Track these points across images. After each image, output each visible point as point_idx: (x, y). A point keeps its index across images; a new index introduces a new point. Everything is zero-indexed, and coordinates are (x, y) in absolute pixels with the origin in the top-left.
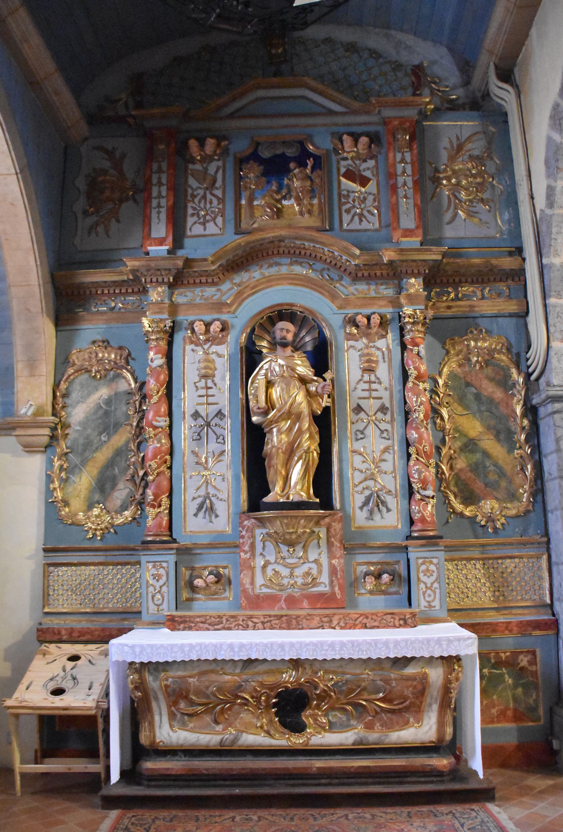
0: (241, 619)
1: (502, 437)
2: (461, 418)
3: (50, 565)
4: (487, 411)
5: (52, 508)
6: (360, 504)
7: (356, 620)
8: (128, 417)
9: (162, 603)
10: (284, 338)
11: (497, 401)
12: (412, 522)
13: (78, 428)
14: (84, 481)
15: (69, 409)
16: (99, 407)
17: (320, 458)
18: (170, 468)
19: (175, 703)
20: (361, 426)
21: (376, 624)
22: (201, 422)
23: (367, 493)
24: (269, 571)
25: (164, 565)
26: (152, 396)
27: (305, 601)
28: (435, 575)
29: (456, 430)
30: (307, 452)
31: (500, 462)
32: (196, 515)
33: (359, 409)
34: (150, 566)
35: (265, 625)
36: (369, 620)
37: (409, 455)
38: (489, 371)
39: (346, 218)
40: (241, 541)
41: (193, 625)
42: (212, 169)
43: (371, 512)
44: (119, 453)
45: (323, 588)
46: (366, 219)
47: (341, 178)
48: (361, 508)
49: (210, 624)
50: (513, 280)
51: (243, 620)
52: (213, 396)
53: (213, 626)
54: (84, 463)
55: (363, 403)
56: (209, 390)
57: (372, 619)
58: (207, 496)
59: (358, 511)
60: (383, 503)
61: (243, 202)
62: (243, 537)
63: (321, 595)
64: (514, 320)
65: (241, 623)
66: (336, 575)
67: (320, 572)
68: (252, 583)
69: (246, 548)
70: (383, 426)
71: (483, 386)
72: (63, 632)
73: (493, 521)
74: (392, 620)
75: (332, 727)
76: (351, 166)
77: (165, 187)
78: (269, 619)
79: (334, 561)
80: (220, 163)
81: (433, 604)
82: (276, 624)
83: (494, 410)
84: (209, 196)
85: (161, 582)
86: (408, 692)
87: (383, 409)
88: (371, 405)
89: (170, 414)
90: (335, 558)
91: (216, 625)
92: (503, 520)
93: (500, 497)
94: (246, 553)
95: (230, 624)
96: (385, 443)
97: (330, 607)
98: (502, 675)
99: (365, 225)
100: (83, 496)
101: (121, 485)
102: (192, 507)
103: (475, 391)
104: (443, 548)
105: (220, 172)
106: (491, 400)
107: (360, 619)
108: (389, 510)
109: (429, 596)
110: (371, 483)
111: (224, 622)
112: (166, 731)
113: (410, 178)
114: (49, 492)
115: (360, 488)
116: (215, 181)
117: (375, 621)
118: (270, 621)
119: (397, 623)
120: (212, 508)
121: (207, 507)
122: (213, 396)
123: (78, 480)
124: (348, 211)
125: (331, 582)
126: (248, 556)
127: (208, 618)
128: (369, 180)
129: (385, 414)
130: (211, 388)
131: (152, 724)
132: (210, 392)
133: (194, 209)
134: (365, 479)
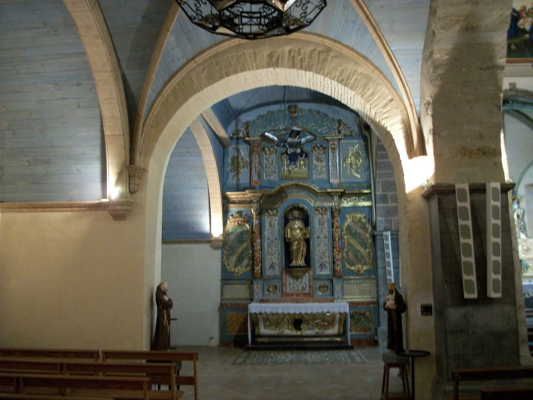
3: (223, 284)
5: (224, 267)
12: (334, 272)
14: (234, 258)
16: (238, 235)
19: (266, 322)
20: (319, 242)
24: (291, 286)
29: (348, 243)
30: (303, 250)
33: (318, 237)
37: (333, 252)
38: (360, 224)
42: (272, 156)
43: (322, 269)
44: (245, 250)
45: (307, 290)
54: (234, 253)
55: (320, 236)
58: (272, 264)
60: (326, 266)
75: (309, 329)
84: (271, 166)
86: (330, 320)
87: (326, 237)
88: (322, 236)
97: (309, 296)
98: (361, 319)
99: (321, 177)
106: (359, 234)
112: (263, 330)
128: (322, 161)
131: (259, 328)
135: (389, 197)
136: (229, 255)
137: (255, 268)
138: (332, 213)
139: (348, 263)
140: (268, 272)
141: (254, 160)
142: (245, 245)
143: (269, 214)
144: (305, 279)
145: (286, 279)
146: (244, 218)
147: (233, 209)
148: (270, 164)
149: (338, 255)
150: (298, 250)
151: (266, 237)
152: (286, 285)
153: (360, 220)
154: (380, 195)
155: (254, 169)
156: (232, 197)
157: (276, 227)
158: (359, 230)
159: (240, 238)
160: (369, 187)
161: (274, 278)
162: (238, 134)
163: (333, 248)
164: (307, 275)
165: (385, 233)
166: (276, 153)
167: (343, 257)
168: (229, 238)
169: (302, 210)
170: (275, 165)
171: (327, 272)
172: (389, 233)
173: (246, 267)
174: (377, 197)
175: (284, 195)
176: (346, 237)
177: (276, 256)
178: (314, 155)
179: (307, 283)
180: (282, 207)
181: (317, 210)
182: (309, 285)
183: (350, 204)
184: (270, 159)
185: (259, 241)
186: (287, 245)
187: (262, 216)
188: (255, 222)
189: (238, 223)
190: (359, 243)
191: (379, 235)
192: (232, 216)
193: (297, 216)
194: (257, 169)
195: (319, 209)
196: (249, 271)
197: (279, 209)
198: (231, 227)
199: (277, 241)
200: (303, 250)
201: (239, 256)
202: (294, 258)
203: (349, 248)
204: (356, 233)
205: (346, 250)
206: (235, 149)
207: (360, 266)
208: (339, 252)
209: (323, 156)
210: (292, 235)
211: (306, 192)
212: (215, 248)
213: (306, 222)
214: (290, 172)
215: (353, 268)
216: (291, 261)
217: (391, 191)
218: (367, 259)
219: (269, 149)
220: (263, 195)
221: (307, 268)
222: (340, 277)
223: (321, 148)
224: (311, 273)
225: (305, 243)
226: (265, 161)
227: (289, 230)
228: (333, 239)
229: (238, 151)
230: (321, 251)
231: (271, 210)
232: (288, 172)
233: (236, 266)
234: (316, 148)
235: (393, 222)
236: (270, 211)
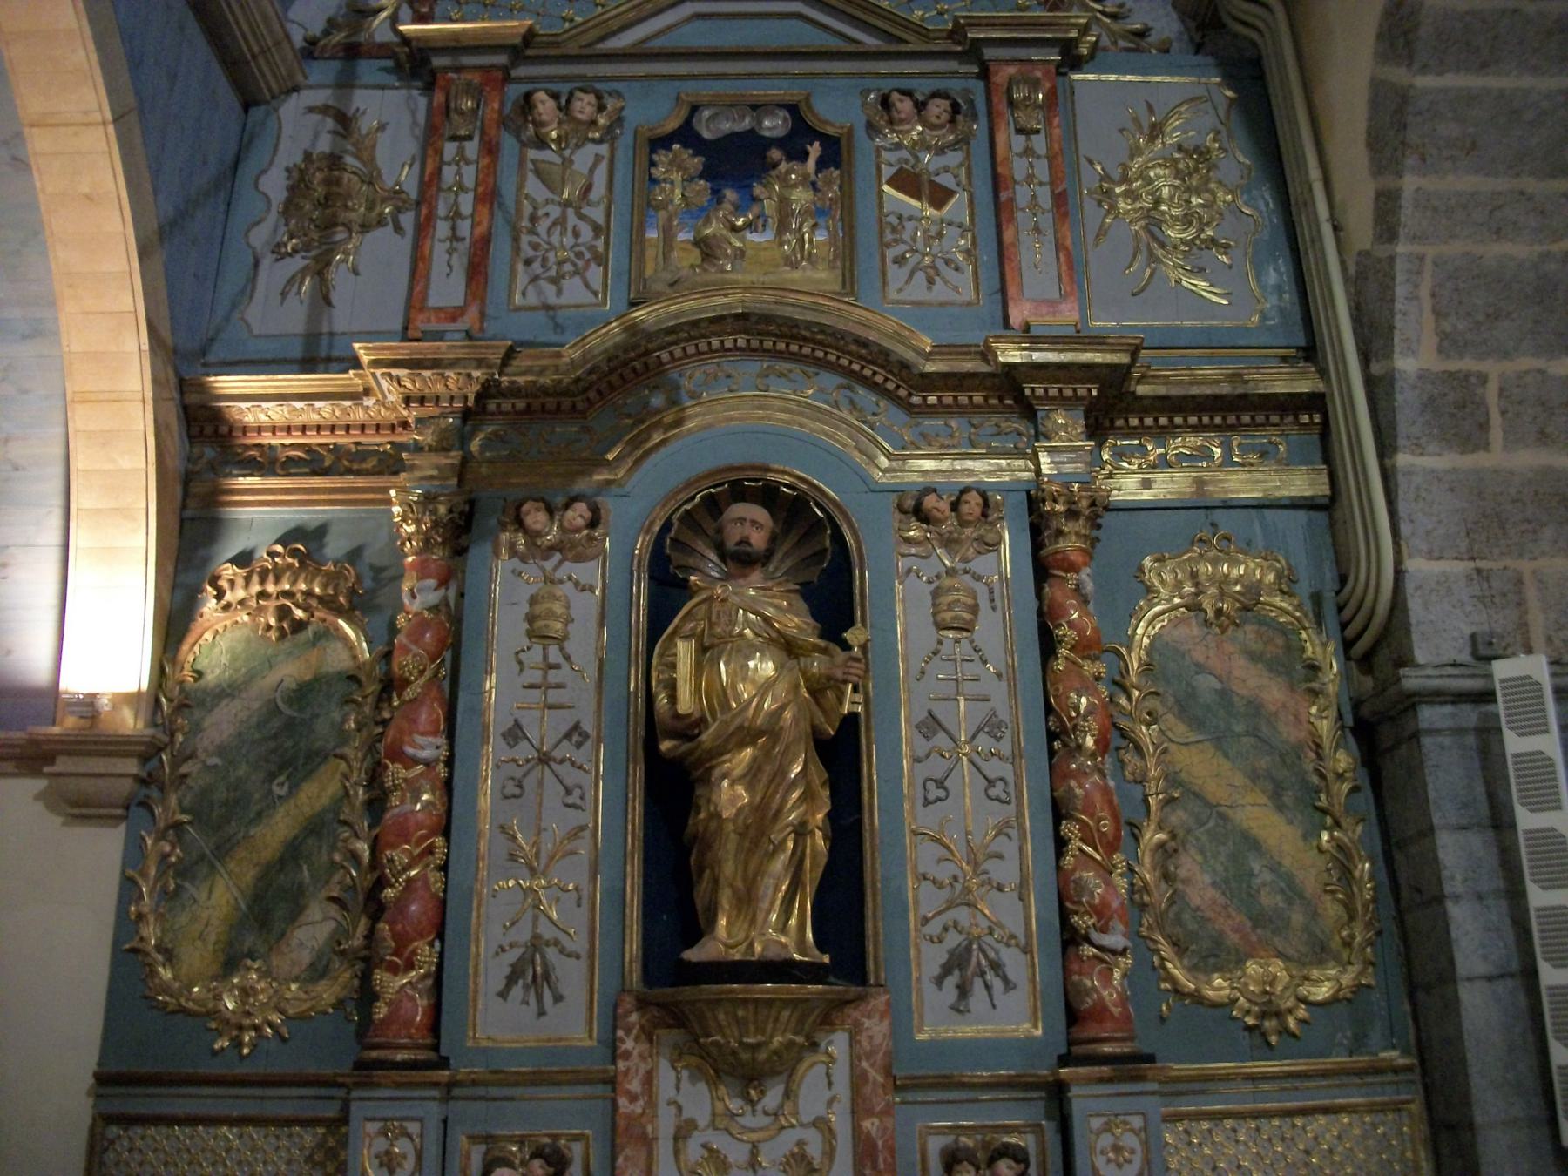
1: (1288, 798)
2: (1184, 749)
4: (1248, 734)
6: (937, 971)
8: (344, 737)
10: (745, 541)
11: (1272, 708)
12: (1073, 1016)
14: (219, 899)
15: (197, 714)
16: (273, 710)
17: (831, 851)
18: (444, 868)
20: (936, 767)
22: (524, 751)
23: (953, 940)
24: (693, 1151)
25: (413, 1128)
26: (406, 683)
28: (1138, 1160)
29: (1172, 780)
30: (801, 831)
31: (1287, 862)
32: (503, 995)
33: (931, 725)
34: (372, 1127)
37: (1061, 844)
38: (1248, 634)
39: (896, 274)
42: (583, 158)
43: (963, 991)
44: (315, 827)
46: (943, 279)
47: (886, 188)
48: (939, 981)
52: (559, 686)
54: (223, 850)
55: (939, 710)
56: (552, 672)
58: (536, 944)
59: (929, 988)
60: (996, 966)
61: (652, 234)
64: (1302, 515)
67: (830, 1154)
69: (635, 1086)
70: (994, 768)
71: (1236, 673)
73: (1279, 1015)
76: (906, 161)
77: (471, 195)
80: (604, 149)
83: (1265, 731)
87: (991, 726)
89: (451, 734)
90: (870, 1113)
92: (1302, 1012)
94: (633, 1098)
96: (996, 814)
99: (940, 292)
100: (213, 938)
101: (315, 911)
102: (493, 973)
103: (1218, 686)
104: (1154, 1086)
105: (603, 168)
106: (1255, 708)
108: (1008, 985)
110: (962, 915)
113: (1047, 188)
114: (126, 924)
115: (934, 928)
116: (588, 188)
120: (547, 976)
121: (530, 973)
122: (559, 686)
123: (204, 895)
124: (900, 261)
126: (638, 1108)
128: (950, 194)
129: (998, 739)
130: (557, 667)
132: (553, 676)
133: (535, 247)
135: (1491, 393)
136: (185, 872)
137: (378, 975)
138: (1038, 529)
139: (1180, 947)
140: (496, 1022)
141: (449, 173)
142: (317, 793)
143: (533, 536)
144: (823, 1088)
145: (649, 1080)
146: (332, 579)
147: (259, 511)
148: (567, 204)
149: (1106, 871)
150: (761, 818)
151: (496, 721)
152: (648, 1142)
153: (1250, 602)
154: (1423, 375)
155: (442, 229)
156: (250, 414)
157: (586, 641)
158: (1252, 681)
159: (288, 734)
160: (1310, 352)
161: (549, 1073)
162: (356, 29)
163: (1059, 811)
164: (837, 1044)
165: (1502, 670)
166: (609, 136)
167: (1138, 901)
168: (197, 729)
169: (796, 513)
170: (598, 215)
171: (1013, 1018)
172: (1536, 667)
173: (317, 971)
174: (1406, 400)
175: (657, 401)
176: (1146, 733)
177: (573, 873)
178: (881, 154)
179: (840, 1120)
180: (639, 492)
181: (920, 514)
182: (856, 1129)
183: (1168, 486)
184: (573, 184)
185: (428, 747)
186: (670, 778)
187: (478, 553)
188: (417, 596)
189: (283, 613)
190: (1254, 777)
191: (1437, 696)
192: (244, 559)
193: (758, 540)
194: (465, 228)
195: (930, 501)
196: (339, 1004)
197: (607, 503)
198: (224, 643)
199: (580, 756)
200: (801, 831)
201: (270, 872)
202: (725, 899)
203: (1178, 817)
205: (1153, 836)
206: (324, 110)
207: (1277, 968)
208: (1112, 847)
209: (954, 158)
210: (720, 698)
211: (830, 380)
212: (81, 809)
213: (833, 600)
214: (707, 249)
215: (1218, 986)
216: (694, 928)
217: (1506, 355)
218: (1332, 910)
219: (565, 109)
220: (488, 391)
221: (839, 988)
222: (1131, 1066)
223: (938, 109)
224: (876, 1029)
225: (819, 774)
226: (533, 186)
227: (685, 652)
228: (1058, 736)
229: (344, 122)
230: (954, 838)
231: (550, 511)
232: (695, 256)
233: (230, 963)
234: (904, 106)
235: (1531, 593)
236: (535, 518)
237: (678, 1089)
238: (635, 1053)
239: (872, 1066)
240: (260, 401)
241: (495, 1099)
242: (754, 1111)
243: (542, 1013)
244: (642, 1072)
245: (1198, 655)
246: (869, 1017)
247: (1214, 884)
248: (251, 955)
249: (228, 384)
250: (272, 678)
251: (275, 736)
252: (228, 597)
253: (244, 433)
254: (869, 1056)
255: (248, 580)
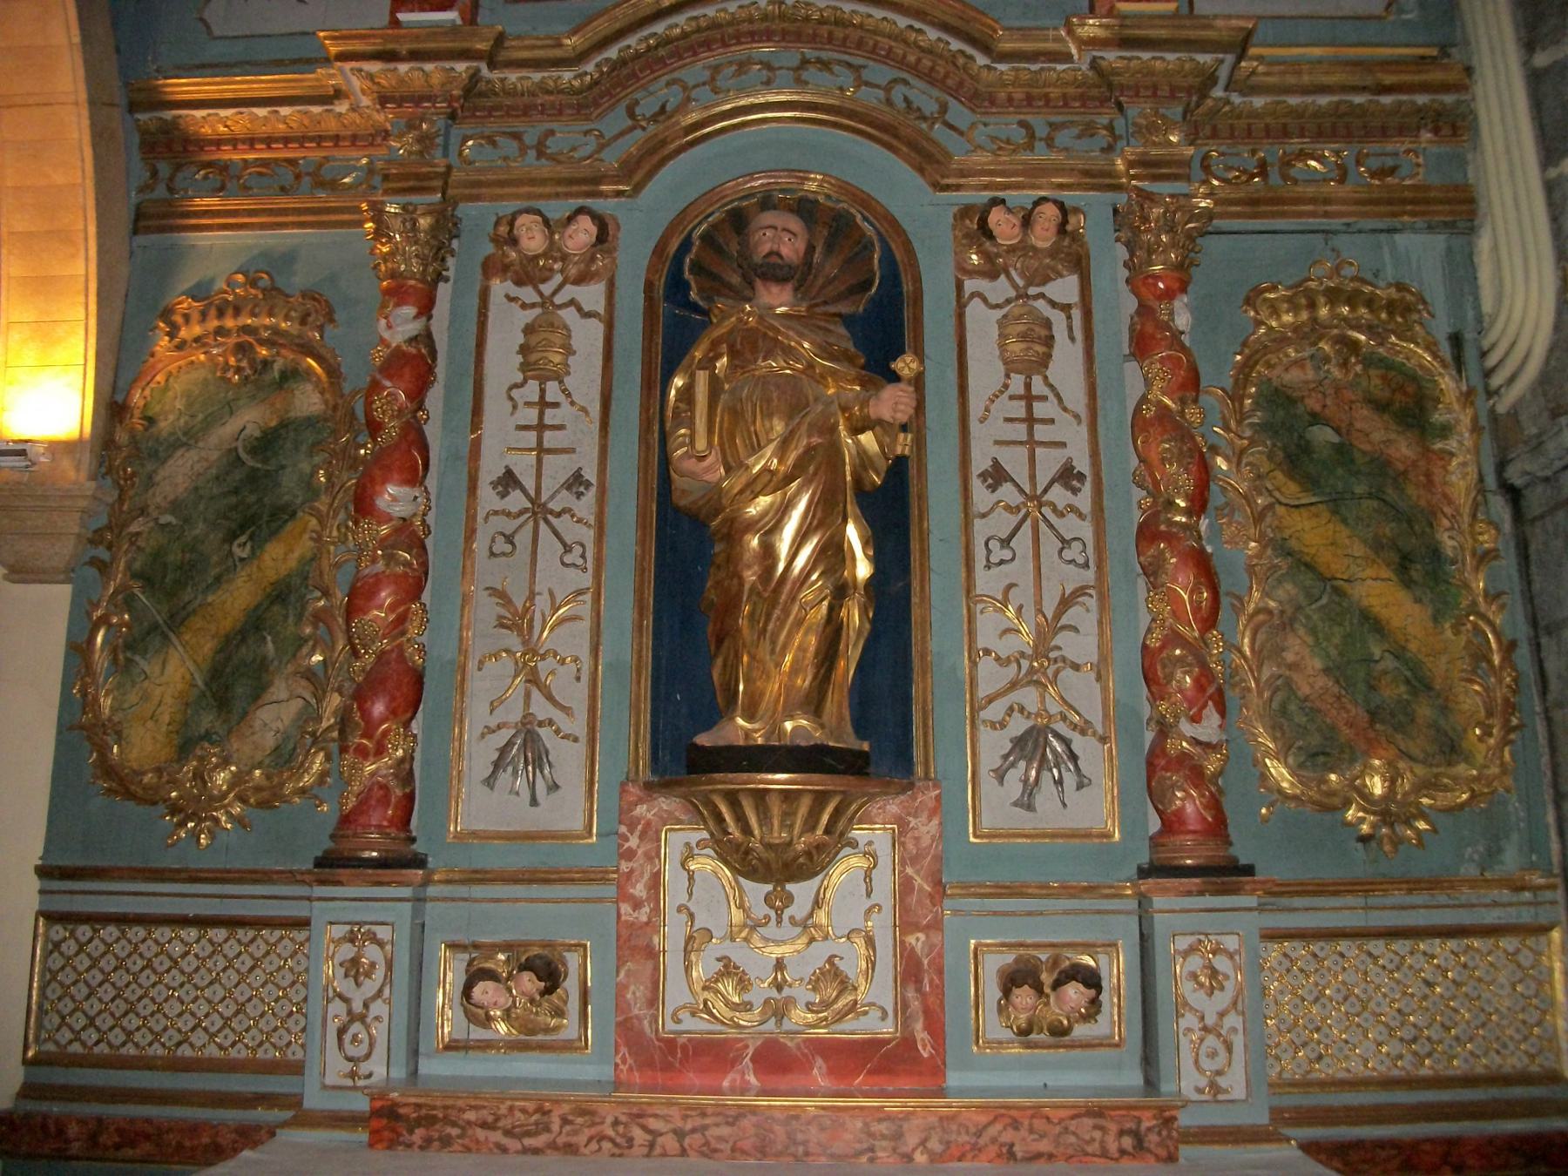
0: (609, 1120)
1: (1416, 572)
2: (1296, 512)
4: (1370, 496)
7: (979, 1134)
9: (368, 1056)
11: (1401, 467)
13: (168, 518)
14: (174, 672)
21: (1044, 1146)
22: (516, 501)
23: (1018, 726)
25: (383, 933)
27: (819, 1061)
32: (490, 782)
35: (687, 1141)
36: (1024, 1133)
40: (625, 866)
41: (455, 1132)
45: (876, 1015)
49: (508, 1133)
50: (1436, 131)
51: (616, 1123)
52: (560, 427)
53: (519, 1137)
54: (177, 620)
56: (549, 412)
57: (1031, 1131)
62: (630, 855)
63: (873, 1045)
65: (611, 1133)
66: (918, 982)
68: (653, 1001)
71: (1358, 425)
72: (73, 1130)
74: (1097, 1134)
78: (698, 1122)
79: (911, 939)
81: (1222, 1082)
82: (720, 1139)
83: (1391, 493)
85: (370, 986)
90: (916, 927)
91: (528, 1134)
93: (1416, 752)
94: (637, 905)
95: (575, 1133)
100: (167, 718)
101: (279, 690)
102: (479, 756)
103: (1336, 439)
106: (1381, 467)
107: (993, 1131)
109: (1213, 1055)
110: (1028, 697)
111: (555, 1127)
117: (1042, 1136)
118: (705, 1128)
119: (1113, 1147)
122: (560, 427)
123: (157, 669)
125: (902, 1006)
126: (643, 915)
127: (503, 1110)
129: (1075, 491)
130: (556, 405)
132: (551, 417)
134: (1013, 685)
156: (204, 122)
168: (150, 482)
190: (1377, 546)
198: (177, 387)
201: (232, 642)
204: (1342, 451)
237: (691, 895)
238: (640, 852)
239: (918, 872)
240: (218, 108)
241: (476, 901)
242: (779, 922)
243: (534, 802)
244: (646, 876)
245: (1313, 403)
246: (916, 817)
247: (1327, 671)
248: (207, 736)
249: (183, 87)
250: (231, 427)
251: (236, 491)
252: (184, 333)
253: (202, 149)
254: (915, 860)
255: (204, 316)
